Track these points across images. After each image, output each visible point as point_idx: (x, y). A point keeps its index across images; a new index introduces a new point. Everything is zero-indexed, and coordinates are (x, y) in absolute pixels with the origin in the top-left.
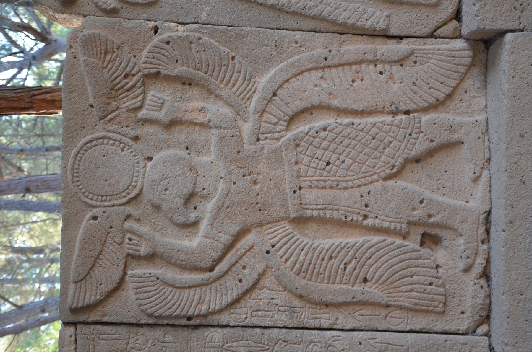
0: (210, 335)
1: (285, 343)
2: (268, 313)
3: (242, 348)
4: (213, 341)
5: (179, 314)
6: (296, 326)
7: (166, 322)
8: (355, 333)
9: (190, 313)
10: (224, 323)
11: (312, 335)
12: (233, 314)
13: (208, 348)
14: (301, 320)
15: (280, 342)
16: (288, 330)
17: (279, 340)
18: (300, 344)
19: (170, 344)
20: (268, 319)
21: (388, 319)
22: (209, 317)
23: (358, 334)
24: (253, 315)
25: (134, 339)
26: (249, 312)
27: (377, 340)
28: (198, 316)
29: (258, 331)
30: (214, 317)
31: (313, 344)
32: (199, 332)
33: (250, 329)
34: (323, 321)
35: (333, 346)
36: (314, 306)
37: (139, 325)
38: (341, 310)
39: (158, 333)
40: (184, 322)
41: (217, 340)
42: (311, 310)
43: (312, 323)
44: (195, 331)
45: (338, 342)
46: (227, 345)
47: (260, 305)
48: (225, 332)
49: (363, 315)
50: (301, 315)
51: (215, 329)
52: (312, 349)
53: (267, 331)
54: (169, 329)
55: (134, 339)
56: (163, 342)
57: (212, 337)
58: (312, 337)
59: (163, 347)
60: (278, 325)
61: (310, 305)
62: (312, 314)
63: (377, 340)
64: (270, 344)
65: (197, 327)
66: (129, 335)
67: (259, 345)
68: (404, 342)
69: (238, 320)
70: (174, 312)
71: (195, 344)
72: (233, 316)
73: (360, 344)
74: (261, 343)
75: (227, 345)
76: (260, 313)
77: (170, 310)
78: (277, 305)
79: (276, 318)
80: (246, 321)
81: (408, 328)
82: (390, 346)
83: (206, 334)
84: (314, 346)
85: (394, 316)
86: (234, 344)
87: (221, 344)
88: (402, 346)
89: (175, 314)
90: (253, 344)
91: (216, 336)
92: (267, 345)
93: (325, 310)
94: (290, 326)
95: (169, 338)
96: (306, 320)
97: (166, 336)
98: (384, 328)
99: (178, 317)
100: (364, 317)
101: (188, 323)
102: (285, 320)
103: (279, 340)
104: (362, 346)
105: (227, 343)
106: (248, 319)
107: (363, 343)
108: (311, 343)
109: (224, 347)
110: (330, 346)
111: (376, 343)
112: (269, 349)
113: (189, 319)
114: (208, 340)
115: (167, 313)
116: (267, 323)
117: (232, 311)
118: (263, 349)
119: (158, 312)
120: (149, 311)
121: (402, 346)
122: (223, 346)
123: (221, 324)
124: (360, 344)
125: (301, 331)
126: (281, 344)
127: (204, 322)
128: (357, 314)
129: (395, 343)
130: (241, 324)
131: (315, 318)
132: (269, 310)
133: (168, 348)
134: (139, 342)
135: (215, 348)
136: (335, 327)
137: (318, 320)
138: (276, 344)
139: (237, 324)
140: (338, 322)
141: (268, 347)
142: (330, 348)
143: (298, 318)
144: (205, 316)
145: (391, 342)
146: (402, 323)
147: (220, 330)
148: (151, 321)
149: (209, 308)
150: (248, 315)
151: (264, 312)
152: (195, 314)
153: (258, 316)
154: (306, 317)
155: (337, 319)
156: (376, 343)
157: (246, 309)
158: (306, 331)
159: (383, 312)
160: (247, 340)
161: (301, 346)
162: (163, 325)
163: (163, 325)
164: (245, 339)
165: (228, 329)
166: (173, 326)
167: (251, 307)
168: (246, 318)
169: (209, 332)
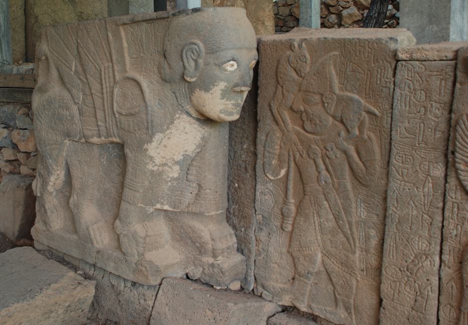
0: (439, 167)
1: (429, 224)
2: (455, 216)
3: (427, 190)
4: (434, 169)
5: (456, 146)
6: (444, 234)
7: (452, 134)
8: (437, 278)
9: (457, 155)
10: (448, 180)
11: (435, 245)
12: (456, 188)
13: (429, 164)
14: (449, 240)
15: (431, 220)
16: (440, 227)
17: (432, 220)
18: (428, 234)
19: (433, 135)
20: (451, 215)
21: (449, 306)
22: (453, 169)
23: (436, 280)
24: (454, 204)
25: (439, 107)
26: (457, 201)
27: (430, 293)
28: (454, 162)
29: (441, 205)
30: (453, 173)
31: (428, 244)
32: (442, 158)
33: (442, 199)
34: (448, 256)
35: (426, 259)
36: (460, 253)
37: (451, 111)
38: (457, 273)
39: (443, 126)
40: (451, 148)
41: (434, 172)
42: (457, 249)
43: (446, 248)
44: (443, 155)
45: (429, 263)
46: (430, 179)
47: (463, 210)
48: (441, 179)
49: (452, 288)
50: (453, 241)
51: (444, 171)
52: (424, 243)
53: (440, 211)
54: (446, 136)
55: (439, 107)
56: (435, 130)
57: (437, 168)
58: (434, 245)
59: (432, 130)
60: (445, 222)
61: (462, 250)
62: (454, 250)
63: (430, 293)
64: (429, 213)
65: (446, 156)
66: (443, 103)
67: (429, 204)
68: (428, 312)
69: (450, 191)
70: (459, 142)
71: (432, 155)
72: (454, 188)
73: (428, 280)
74: (430, 205)
75: (430, 179)
76: (456, 209)
77: (461, 140)
78: (463, 224)
79: (451, 220)
80: (449, 198)
81: (440, 318)
82: (425, 301)
83: (441, 164)
84: (427, 245)
85: (451, 312)
86: (431, 185)
87: (432, 174)
88: (425, 310)
89: (457, 143)
90: (430, 199)
91: (438, 171)
92: (429, 210)
93: (457, 261)
94: (443, 230)
95: (438, 135)
96: (449, 244)
97: (440, 133)
98: (441, 301)
99: (455, 145)
100: (451, 289)
101: (450, 152)
102: (449, 228)
103: (432, 220)
104: (425, 281)
105: (432, 179)
106: (451, 199)
107: (428, 282)
108: (429, 243)
109: (429, 177)
110: (426, 257)
111: (428, 291)
112: (425, 210)
113: (453, 153)
114: (435, 165)
115: (458, 137)
116: (447, 214)
117: (458, 187)
118: (426, 206)
119: (460, 129)
120: (461, 122)
121: (425, 310)
122: (430, 176)
123: (448, 177)
124: (428, 280)
125: (440, 238)
126: (429, 220)
127: (450, 164)
128: (453, 284)
129: (427, 306)
130: (447, 193)
131: (450, 251)
132: (459, 217)
133: (430, 133)
134: (437, 111)
135: (428, 170)
136: (443, 264)
137: (448, 253)
138: (430, 217)
139: (447, 190)
140: (447, 268)
141: (427, 210)
142: (424, 257)
143: (450, 238)
144: (454, 166)
145: (428, 302)
146: (446, 315)
147: (443, 175)
148: (453, 122)
149: (461, 171)
150: (454, 200)
151: (456, 213)
152: (457, 160)
153: (453, 207)
154: (451, 245)
155: (449, 268)
156: (428, 291)
157: (460, 199)
158: (439, 241)
159: (454, 304)
160: (433, 195)
161: (427, 235)
162: (449, 131)
163: (449, 131)
164: (434, 194)
165: (443, 182)
166: (448, 140)
167: (461, 203)
168: (452, 198)
169: (442, 166)
